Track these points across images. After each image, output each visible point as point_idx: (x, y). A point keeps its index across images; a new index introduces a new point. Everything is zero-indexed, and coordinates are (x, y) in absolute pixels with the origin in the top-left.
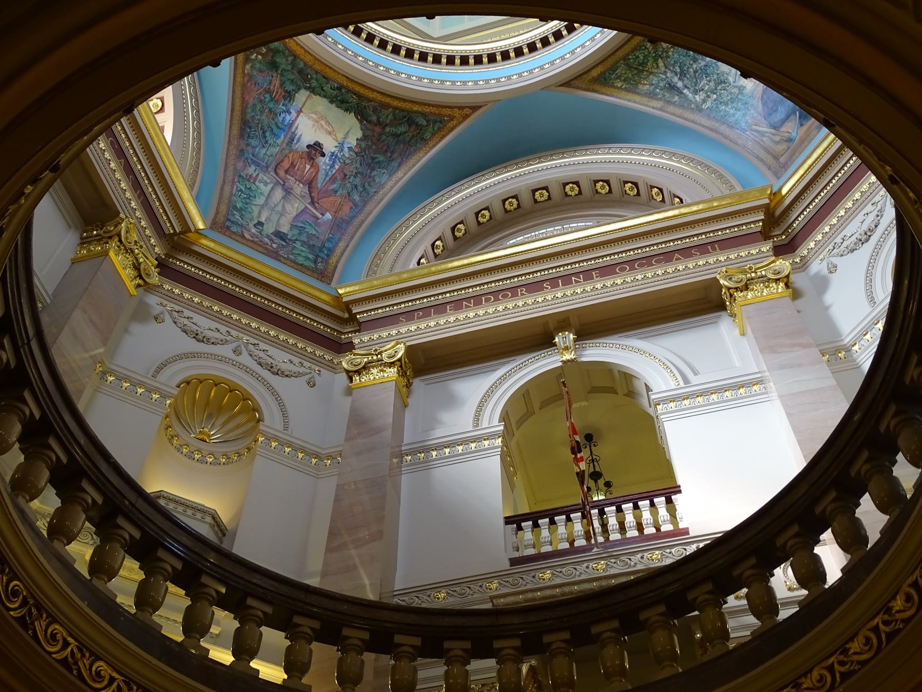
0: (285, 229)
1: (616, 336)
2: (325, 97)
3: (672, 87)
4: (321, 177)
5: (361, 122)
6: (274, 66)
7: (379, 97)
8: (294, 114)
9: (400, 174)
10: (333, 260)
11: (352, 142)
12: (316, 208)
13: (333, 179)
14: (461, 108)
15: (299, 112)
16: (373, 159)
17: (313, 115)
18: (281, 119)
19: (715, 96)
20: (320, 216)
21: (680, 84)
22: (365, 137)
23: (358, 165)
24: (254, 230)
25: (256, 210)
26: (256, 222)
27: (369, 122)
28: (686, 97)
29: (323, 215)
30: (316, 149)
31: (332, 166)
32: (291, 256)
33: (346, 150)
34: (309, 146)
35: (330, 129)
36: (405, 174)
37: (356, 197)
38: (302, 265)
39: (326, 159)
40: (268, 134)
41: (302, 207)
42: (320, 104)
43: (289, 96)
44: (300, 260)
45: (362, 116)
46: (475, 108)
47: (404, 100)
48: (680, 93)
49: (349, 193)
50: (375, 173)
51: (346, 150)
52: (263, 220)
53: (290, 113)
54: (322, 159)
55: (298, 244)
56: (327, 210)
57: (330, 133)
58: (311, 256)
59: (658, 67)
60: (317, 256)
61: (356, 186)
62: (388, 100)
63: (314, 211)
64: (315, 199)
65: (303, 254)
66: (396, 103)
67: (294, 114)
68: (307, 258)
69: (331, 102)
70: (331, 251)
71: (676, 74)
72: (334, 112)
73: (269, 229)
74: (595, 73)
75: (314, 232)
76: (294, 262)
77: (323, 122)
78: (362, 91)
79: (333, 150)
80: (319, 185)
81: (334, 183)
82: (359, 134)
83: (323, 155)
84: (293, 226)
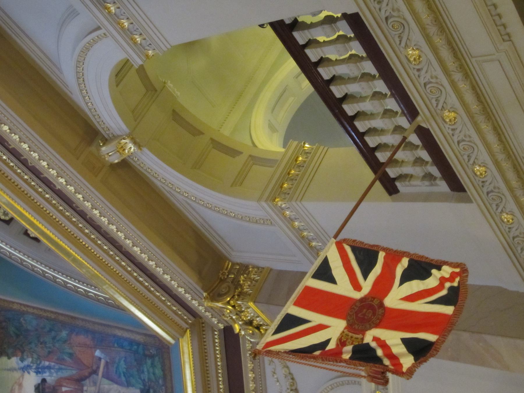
1: (79, 107)
4: (66, 374)
9: (15, 307)
11: (14, 362)
12: (98, 368)
13: (60, 361)
16: (18, 336)
20: (103, 362)
23: (33, 345)
29: (100, 359)
31: (49, 368)
32: (161, 382)
33: (26, 363)
35: (17, 387)
36: (13, 303)
37: (64, 334)
38: (163, 370)
39: (46, 375)
41: (105, 381)
44: (158, 372)
49: (65, 342)
50: (29, 328)
51: (26, 363)
54: (49, 379)
55: (145, 376)
56: (93, 356)
57: (20, 385)
58: (149, 362)
60: (145, 356)
61: (54, 338)
64: (90, 370)
65: (151, 370)
70: (132, 342)
75: (122, 362)
76: (164, 377)
79: (33, 374)
80: (74, 372)
81: (63, 359)
83: (44, 381)
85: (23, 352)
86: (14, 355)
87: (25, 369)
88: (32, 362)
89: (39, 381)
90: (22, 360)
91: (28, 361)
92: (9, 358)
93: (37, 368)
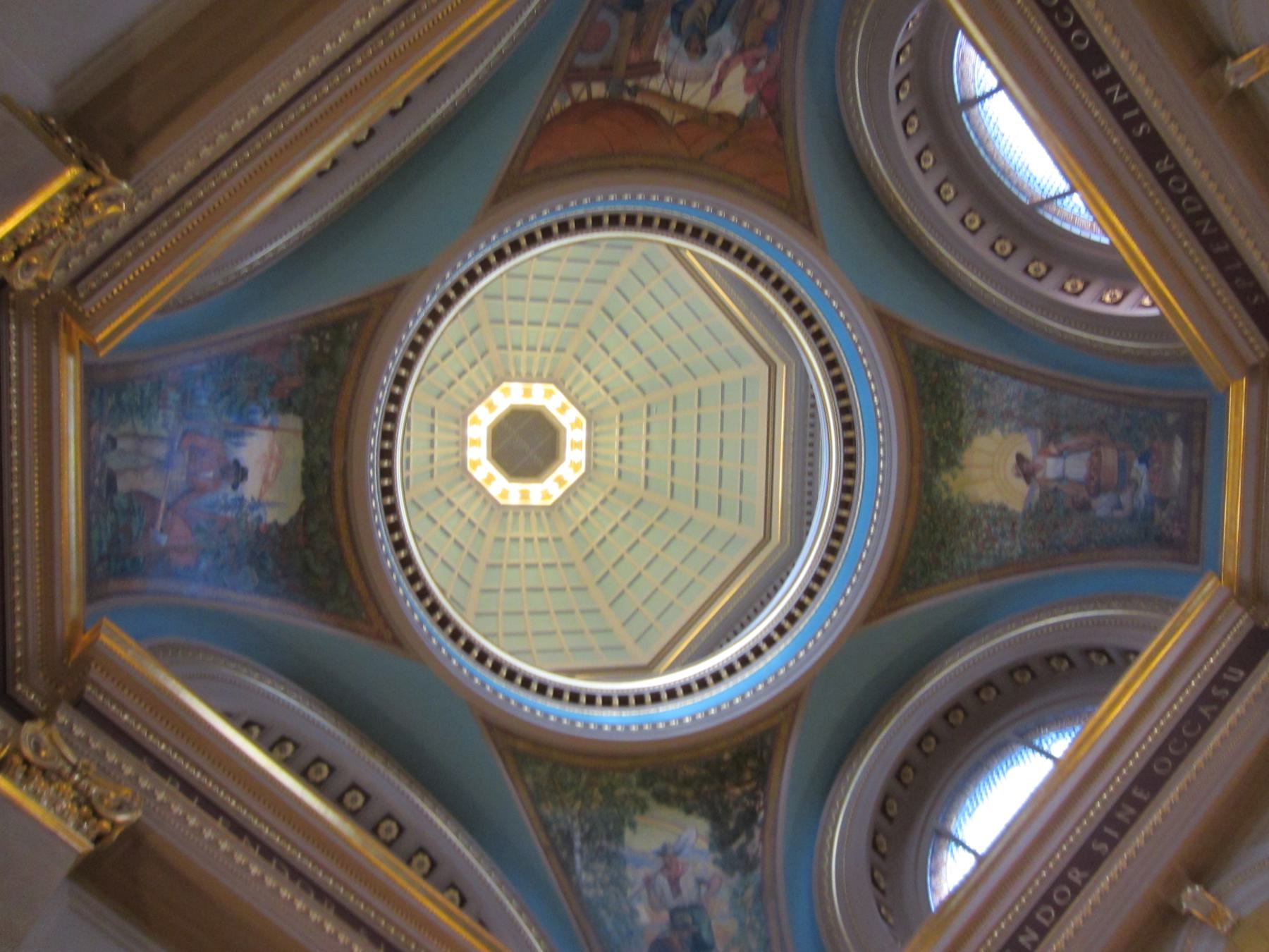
0: (122, 485)
2: (307, 451)
3: (568, 838)
5: (299, 513)
6: (313, 369)
7: (342, 520)
8: (267, 422)
9: (266, 602)
10: (114, 585)
11: (270, 516)
14: (387, 625)
15: (272, 428)
17: (276, 449)
18: (253, 406)
19: (601, 892)
20: (158, 527)
21: (577, 844)
22: (283, 530)
24: (103, 437)
25: (126, 428)
26: (115, 434)
27: (305, 524)
28: (573, 861)
30: (240, 473)
31: (227, 507)
33: (256, 514)
34: (237, 463)
35: (270, 478)
37: (204, 565)
39: (231, 495)
40: (227, 399)
42: (296, 450)
43: (286, 405)
45: (307, 511)
46: (397, 642)
47: (356, 551)
48: (571, 851)
51: (256, 514)
52: (122, 444)
53: (266, 414)
54: (229, 489)
55: (111, 517)
57: (265, 480)
59: (572, 806)
62: (344, 532)
63: (161, 516)
66: (346, 544)
67: (267, 422)
68: (100, 544)
69: (305, 464)
71: (582, 830)
72: (294, 472)
73: (113, 461)
74: (521, 746)
77: (274, 465)
78: (338, 495)
79: (248, 497)
82: (283, 520)
84: (129, 495)
85: (258, 531)
86: (269, 527)
87: (257, 504)
88: (247, 515)
89: (241, 486)
90: (259, 519)
91: (252, 517)
92: (276, 523)
93: (241, 507)
